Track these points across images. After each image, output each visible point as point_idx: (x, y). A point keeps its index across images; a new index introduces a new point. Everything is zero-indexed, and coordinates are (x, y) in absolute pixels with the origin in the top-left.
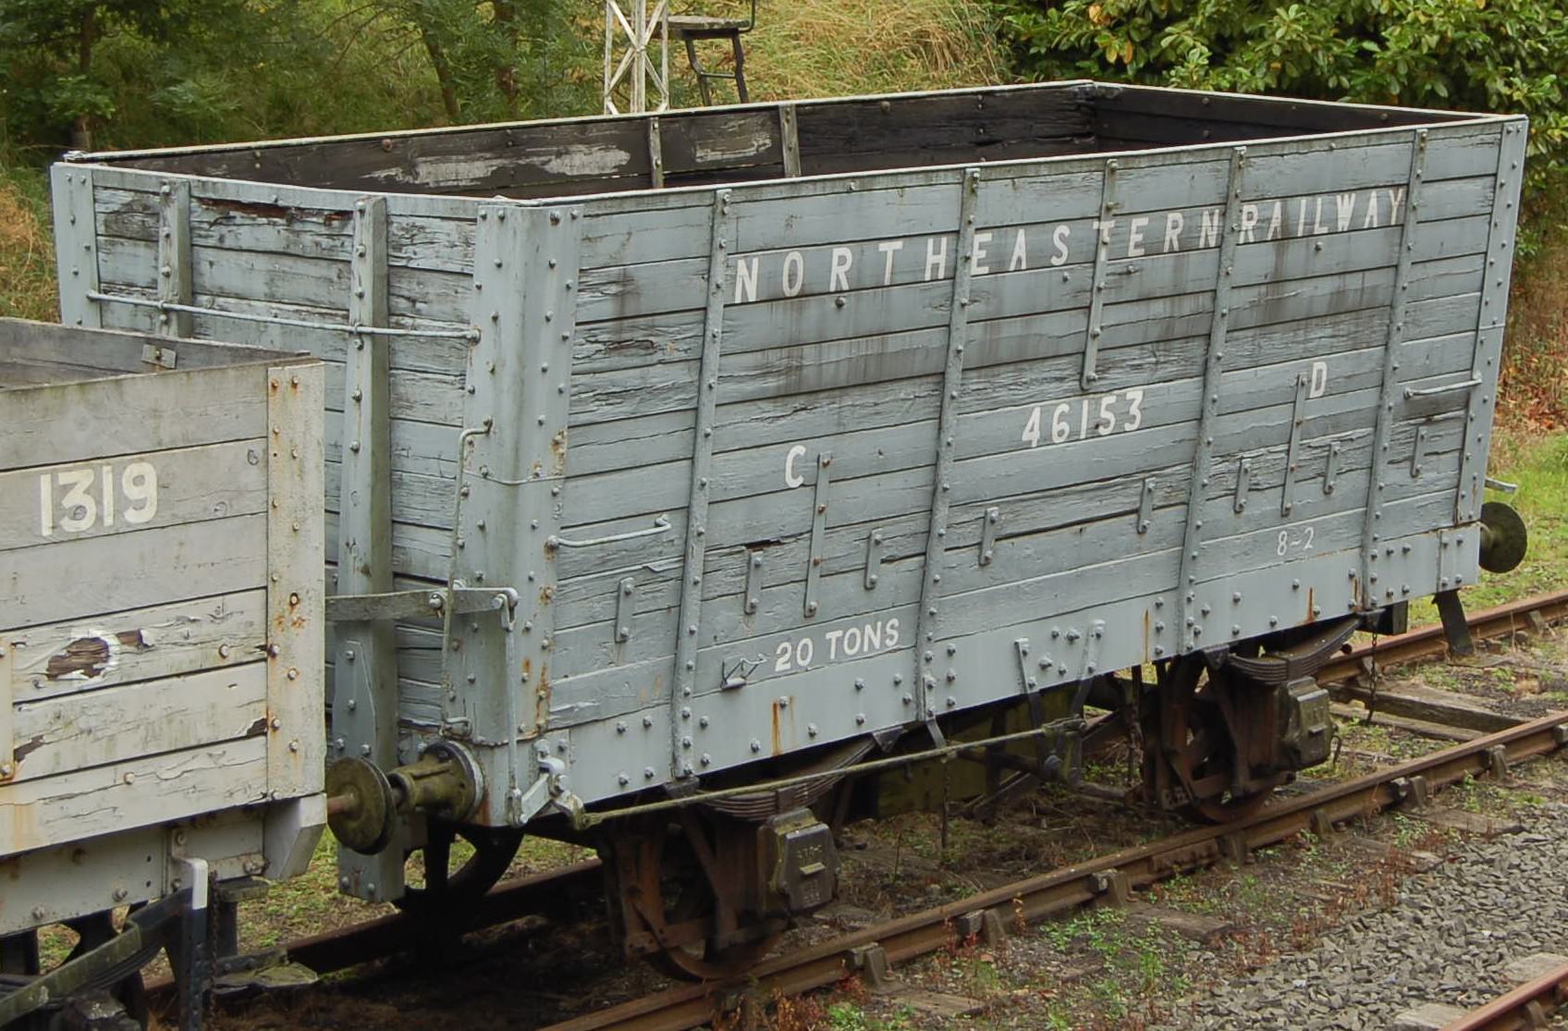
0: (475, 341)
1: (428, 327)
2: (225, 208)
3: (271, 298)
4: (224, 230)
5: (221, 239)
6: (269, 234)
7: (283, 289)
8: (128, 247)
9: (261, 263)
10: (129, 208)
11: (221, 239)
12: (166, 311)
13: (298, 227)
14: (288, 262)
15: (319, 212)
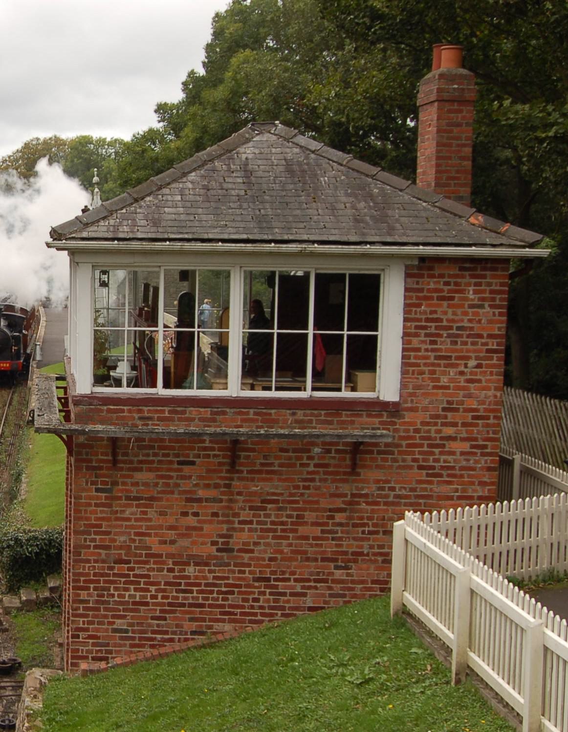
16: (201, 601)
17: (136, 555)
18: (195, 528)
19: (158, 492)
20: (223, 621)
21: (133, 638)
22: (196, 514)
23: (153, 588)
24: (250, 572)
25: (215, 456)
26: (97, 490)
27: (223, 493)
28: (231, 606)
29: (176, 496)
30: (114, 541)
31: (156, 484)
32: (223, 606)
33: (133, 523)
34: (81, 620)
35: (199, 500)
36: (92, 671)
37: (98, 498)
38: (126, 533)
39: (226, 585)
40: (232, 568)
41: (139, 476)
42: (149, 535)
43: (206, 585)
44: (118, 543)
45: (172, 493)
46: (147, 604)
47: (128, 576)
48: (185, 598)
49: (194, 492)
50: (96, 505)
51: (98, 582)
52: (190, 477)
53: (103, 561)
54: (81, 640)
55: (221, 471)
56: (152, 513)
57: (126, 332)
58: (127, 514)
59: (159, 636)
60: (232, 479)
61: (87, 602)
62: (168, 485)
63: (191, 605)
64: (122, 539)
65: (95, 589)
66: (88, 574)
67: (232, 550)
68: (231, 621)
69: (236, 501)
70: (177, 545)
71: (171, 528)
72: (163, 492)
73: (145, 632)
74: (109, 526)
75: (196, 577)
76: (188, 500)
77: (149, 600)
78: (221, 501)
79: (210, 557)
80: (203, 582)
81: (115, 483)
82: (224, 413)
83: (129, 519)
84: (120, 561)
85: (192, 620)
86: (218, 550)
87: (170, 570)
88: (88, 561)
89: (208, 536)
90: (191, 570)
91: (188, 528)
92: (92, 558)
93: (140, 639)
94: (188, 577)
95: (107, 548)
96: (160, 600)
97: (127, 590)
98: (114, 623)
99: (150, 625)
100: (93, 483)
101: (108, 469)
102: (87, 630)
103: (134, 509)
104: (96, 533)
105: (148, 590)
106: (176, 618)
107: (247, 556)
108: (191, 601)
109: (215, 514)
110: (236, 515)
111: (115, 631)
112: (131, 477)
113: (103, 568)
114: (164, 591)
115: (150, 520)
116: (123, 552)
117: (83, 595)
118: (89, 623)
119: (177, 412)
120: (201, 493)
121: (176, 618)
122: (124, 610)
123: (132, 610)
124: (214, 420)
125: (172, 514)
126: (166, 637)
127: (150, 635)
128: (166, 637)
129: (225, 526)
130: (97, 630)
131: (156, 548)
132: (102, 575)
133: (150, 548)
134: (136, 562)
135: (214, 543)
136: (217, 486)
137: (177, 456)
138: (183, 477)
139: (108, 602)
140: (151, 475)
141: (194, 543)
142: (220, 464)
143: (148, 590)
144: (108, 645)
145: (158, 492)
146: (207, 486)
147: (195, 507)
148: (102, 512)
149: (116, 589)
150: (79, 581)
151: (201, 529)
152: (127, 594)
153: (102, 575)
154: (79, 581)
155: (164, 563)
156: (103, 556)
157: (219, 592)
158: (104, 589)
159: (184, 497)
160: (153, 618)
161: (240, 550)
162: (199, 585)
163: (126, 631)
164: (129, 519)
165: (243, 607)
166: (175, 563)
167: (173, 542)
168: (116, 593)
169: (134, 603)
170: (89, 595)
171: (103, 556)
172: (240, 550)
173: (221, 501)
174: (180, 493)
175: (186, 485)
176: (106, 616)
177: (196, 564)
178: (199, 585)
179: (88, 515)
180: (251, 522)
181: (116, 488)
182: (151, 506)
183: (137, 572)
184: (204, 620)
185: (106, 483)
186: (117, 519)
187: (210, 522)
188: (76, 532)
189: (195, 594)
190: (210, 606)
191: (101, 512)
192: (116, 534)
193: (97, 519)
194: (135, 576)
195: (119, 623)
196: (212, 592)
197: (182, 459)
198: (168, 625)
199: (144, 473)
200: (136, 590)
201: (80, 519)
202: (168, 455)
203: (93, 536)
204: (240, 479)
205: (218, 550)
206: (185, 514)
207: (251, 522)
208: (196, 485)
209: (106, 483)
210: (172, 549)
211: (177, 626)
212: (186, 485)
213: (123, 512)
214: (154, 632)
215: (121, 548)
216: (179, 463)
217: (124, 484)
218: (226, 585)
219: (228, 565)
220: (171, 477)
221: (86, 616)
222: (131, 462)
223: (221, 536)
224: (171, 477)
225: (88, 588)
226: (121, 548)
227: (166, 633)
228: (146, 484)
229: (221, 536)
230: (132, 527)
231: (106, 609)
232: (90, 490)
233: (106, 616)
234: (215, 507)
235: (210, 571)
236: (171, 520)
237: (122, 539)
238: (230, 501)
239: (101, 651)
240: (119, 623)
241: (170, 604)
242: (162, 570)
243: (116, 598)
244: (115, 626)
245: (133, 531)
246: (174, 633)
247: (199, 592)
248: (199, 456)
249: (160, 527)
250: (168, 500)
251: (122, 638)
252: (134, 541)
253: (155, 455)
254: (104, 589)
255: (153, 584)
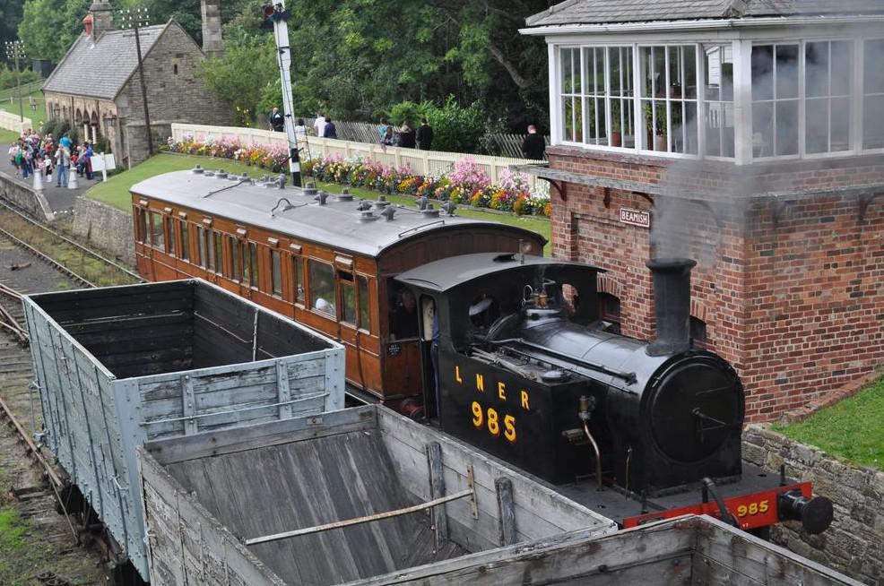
0: (328, 395)
1: (305, 397)
2: (208, 378)
3: (233, 404)
4: (208, 386)
5: (207, 389)
6: (231, 382)
7: (238, 399)
8: (159, 403)
9: (228, 393)
10: (159, 388)
11: (207, 389)
12: (192, 419)
13: (244, 377)
14: (240, 389)
15: (254, 370)
16: (840, 344)
17: (793, 310)
18: (835, 279)
19: (808, 250)
20: (855, 359)
21: (791, 387)
22: (835, 266)
23: (805, 338)
24: (875, 312)
25: (848, 211)
26: (762, 254)
27: (854, 244)
28: (862, 344)
29: (820, 251)
30: (775, 299)
31: (806, 242)
32: (855, 345)
33: (789, 280)
34: (752, 376)
35: (837, 253)
36: (802, 416)
37: (763, 261)
38: (783, 290)
39: (858, 326)
40: (861, 310)
41: (794, 237)
42: (800, 290)
43: (845, 328)
44: (778, 301)
45: (818, 248)
46: (800, 353)
47: (786, 330)
48: (828, 343)
49: (834, 246)
50: (762, 268)
51: (763, 339)
52: (831, 232)
53: (768, 320)
54: (752, 396)
55: (851, 224)
56: (803, 270)
57: (829, 93)
58: (784, 274)
59: (810, 381)
60: (860, 230)
61: (756, 359)
62: (814, 241)
63: (833, 348)
64: (781, 296)
65: (762, 346)
66: (756, 334)
67: (861, 294)
68: (861, 358)
69: (864, 249)
70: (822, 295)
71: (818, 280)
72: (813, 249)
73: (799, 379)
74: (772, 286)
75: (836, 323)
76: (830, 253)
77: (802, 349)
78: (853, 251)
79: (846, 302)
80: (841, 326)
81: (775, 246)
82: (855, 171)
83: (786, 278)
84: (780, 317)
85: (833, 362)
86: (852, 296)
87: (818, 319)
88: (756, 321)
89: (844, 284)
90: (832, 317)
91: (831, 279)
92: (759, 318)
93: (797, 386)
94: (830, 324)
95: (770, 306)
96: (810, 348)
97: (785, 343)
98: (776, 375)
99: (803, 372)
100: (759, 248)
101: (771, 233)
102: (756, 385)
103: (790, 268)
104: (762, 294)
105: (801, 341)
106: (822, 362)
107: (871, 297)
108: (833, 345)
109: (849, 264)
110: (864, 262)
111: (778, 382)
112: (787, 238)
113: (768, 326)
114: (813, 339)
115: (801, 276)
116: (782, 308)
117: (753, 353)
118: (758, 378)
119: (820, 174)
120: (839, 246)
121: (822, 362)
122: (784, 362)
123: (790, 361)
124: (848, 178)
125: (818, 268)
126: (815, 380)
127: (803, 381)
128: (815, 380)
129: (856, 273)
130: (764, 384)
131: (808, 301)
132: (767, 332)
133: (802, 302)
134: (793, 316)
135: (849, 290)
136: (850, 238)
137: (821, 214)
138: (825, 233)
139: (771, 357)
140: (802, 234)
141: (834, 292)
142: (852, 218)
143: (801, 341)
144: (772, 396)
145: (808, 250)
146: (843, 239)
147: (835, 259)
148: (766, 274)
149: (778, 343)
150: (749, 341)
151: (839, 278)
152: (786, 346)
153: (767, 332)
154: (749, 341)
155: (813, 313)
156: (768, 315)
157: (853, 333)
158: (769, 345)
159: (826, 251)
160: (806, 365)
161: (867, 293)
162: (838, 329)
163: (786, 381)
164: (786, 278)
165: (869, 344)
166: (821, 313)
167: (819, 293)
168: (778, 347)
169: (792, 354)
170: (757, 353)
171: (768, 315)
172: (867, 293)
173: (853, 251)
174: (824, 247)
175: (828, 240)
176: (770, 370)
177: (836, 311)
178: (838, 329)
179: (755, 278)
180: (874, 267)
181: (776, 250)
182: (802, 263)
183: (794, 325)
184: (842, 360)
185: (767, 246)
186: (777, 279)
187: (845, 271)
188: (746, 296)
189: (836, 338)
190: (847, 347)
191: (766, 273)
192: (777, 292)
193: (762, 281)
194: (792, 329)
195: (781, 375)
196: (847, 334)
197: (824, 216)
198: (816, 370)
199: (797, 233)
200: (792, 341)
201: (750, 282)
202: (814, 214)
203: (759, 298)
204: (866, 229)
205: (852, 296)
206: (827, 266)
207: (874, 267)
208: (835, 239)
209: (767, 246)
210: (818, 300)
211: (823, 369)
212: (828, 240)
213: (782, 271)
214: (806, 378)
215: (781, 305)
216: (823, 220)
217: (782, 245)
218: (858, 326)
219: (858, 308)
220: (816, 235)
221: (755, 373)
222: (787, 224)
223: (853, 283)
224: (816, 235)
225: (756, 347)
226: (781, 305)
227: (815, 377)
228: (798, 243)
229: (853, 283)
230: (789, 284)
231: (770, 364)
232: (755, 255)
233: (770, 370)
234: (849, 257)
235: (846, 315)
236: (817, 274)
237: (781, 296)
238: (860, 250)
239: (767, 403)
240: (781, 375)
241: (818, 351)
242: (810, 320)
243: (778, 352)
244: (777, 378)
245: (789, 288)
246: (821, 376)
247: (839, 335)
248: (836, 213)
249: (809, 281)
250: (815, 255)
251: (783, 388)
252: (790, 297)
253: (805, 215)
254: (769, 345)
255: (804, 334)
